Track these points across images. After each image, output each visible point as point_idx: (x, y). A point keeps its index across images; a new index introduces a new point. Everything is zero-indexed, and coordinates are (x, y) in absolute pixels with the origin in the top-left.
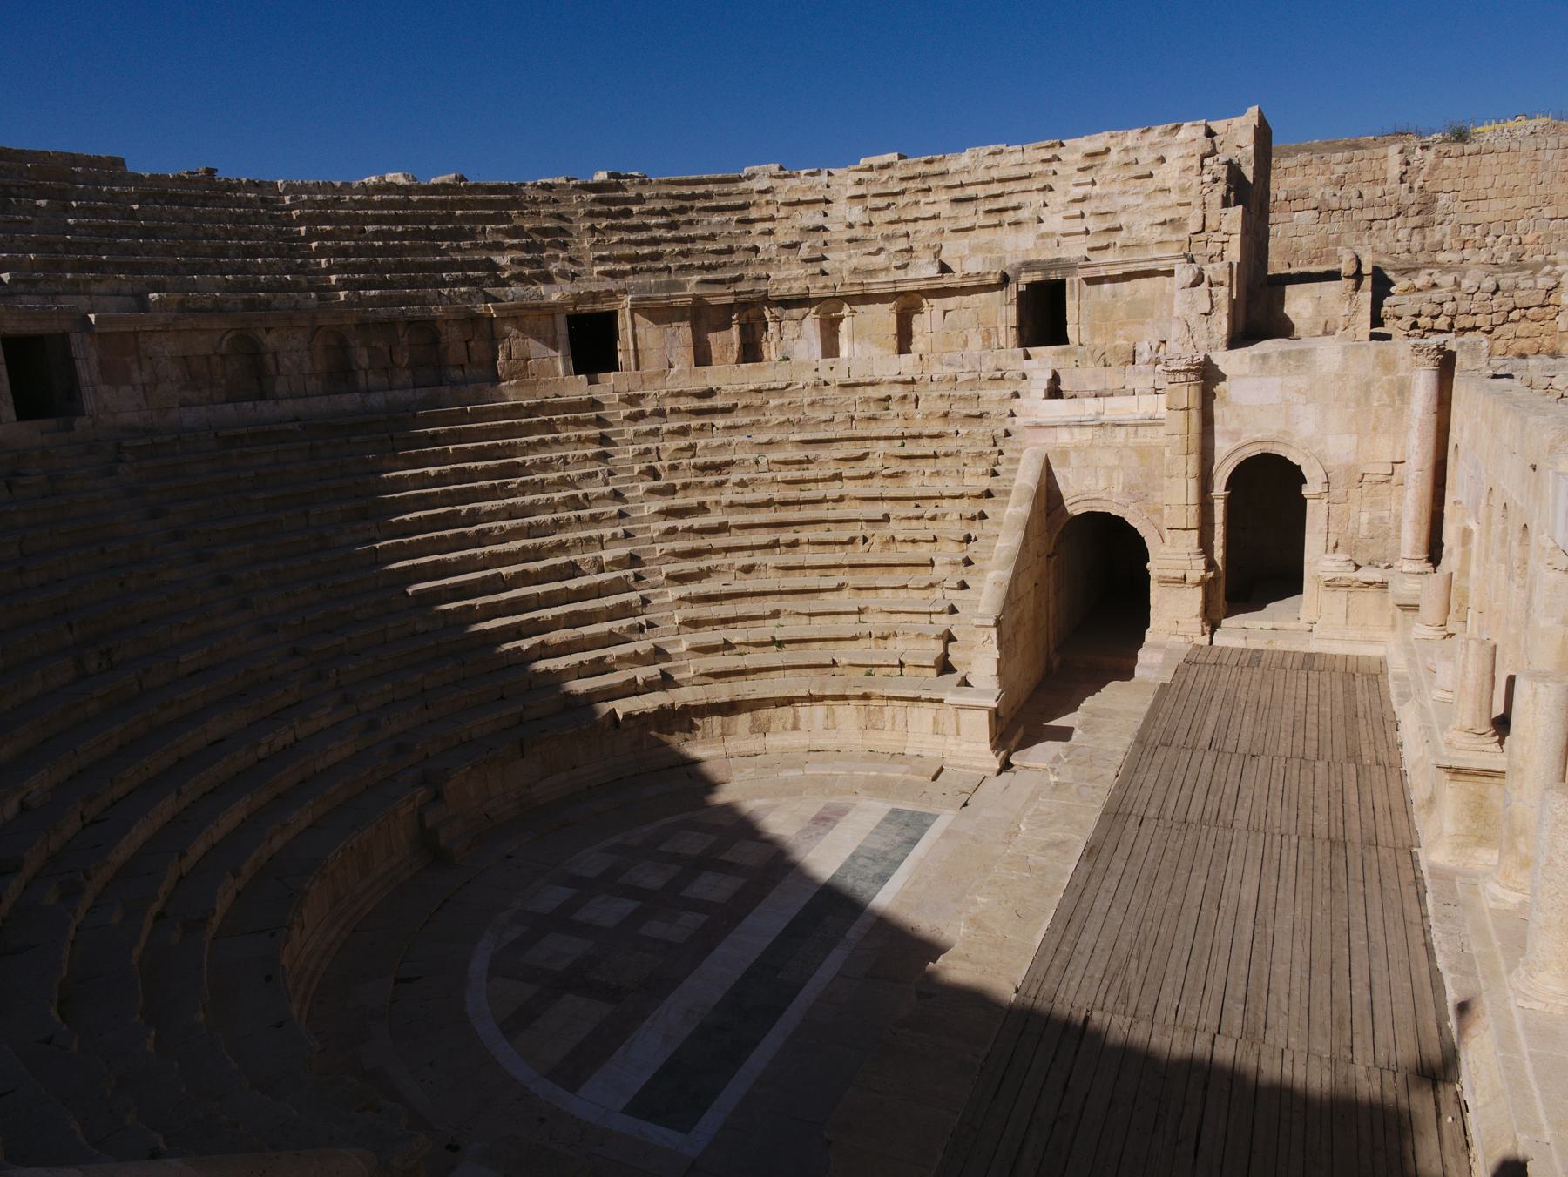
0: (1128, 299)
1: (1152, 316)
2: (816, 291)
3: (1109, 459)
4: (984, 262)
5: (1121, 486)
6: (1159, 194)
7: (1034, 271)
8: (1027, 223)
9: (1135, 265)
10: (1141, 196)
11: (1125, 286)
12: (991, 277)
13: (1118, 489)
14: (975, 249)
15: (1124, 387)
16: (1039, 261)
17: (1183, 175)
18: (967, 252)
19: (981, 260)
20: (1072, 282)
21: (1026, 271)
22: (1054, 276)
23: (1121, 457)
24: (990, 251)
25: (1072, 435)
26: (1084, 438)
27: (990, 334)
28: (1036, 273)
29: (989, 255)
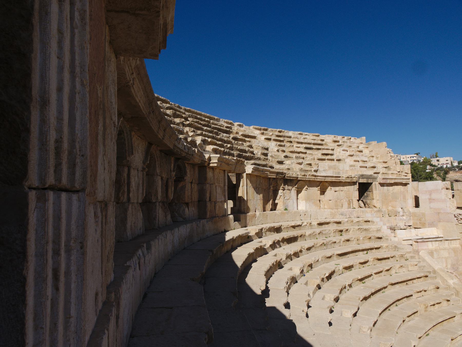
0: (392, 192)
1: (399, 199)
2: (301, 176)
3: (445, 254)
4: (333, 173)
5: (450, 265)
6: (371, 157)
7: (364, 178)
8: (342, 160)
9: (397, 180)
10: (367, 157)
11: (391, 188)
12: (355, 179)
13: (449, 266)
14: (330, 167)
15: (396, 225)
16: (366, 175)
17: (370, 153)
18: (327, 168)
19: (332, 172)
20: (375, 184)
21: (362, 178)
22: (370, 181)
23: (449, 253)
24: (335, 169)
25: (432, 244)
26: (436, 246)
27: (350, 202)
28: (365, 179)
29: (335, 171)
